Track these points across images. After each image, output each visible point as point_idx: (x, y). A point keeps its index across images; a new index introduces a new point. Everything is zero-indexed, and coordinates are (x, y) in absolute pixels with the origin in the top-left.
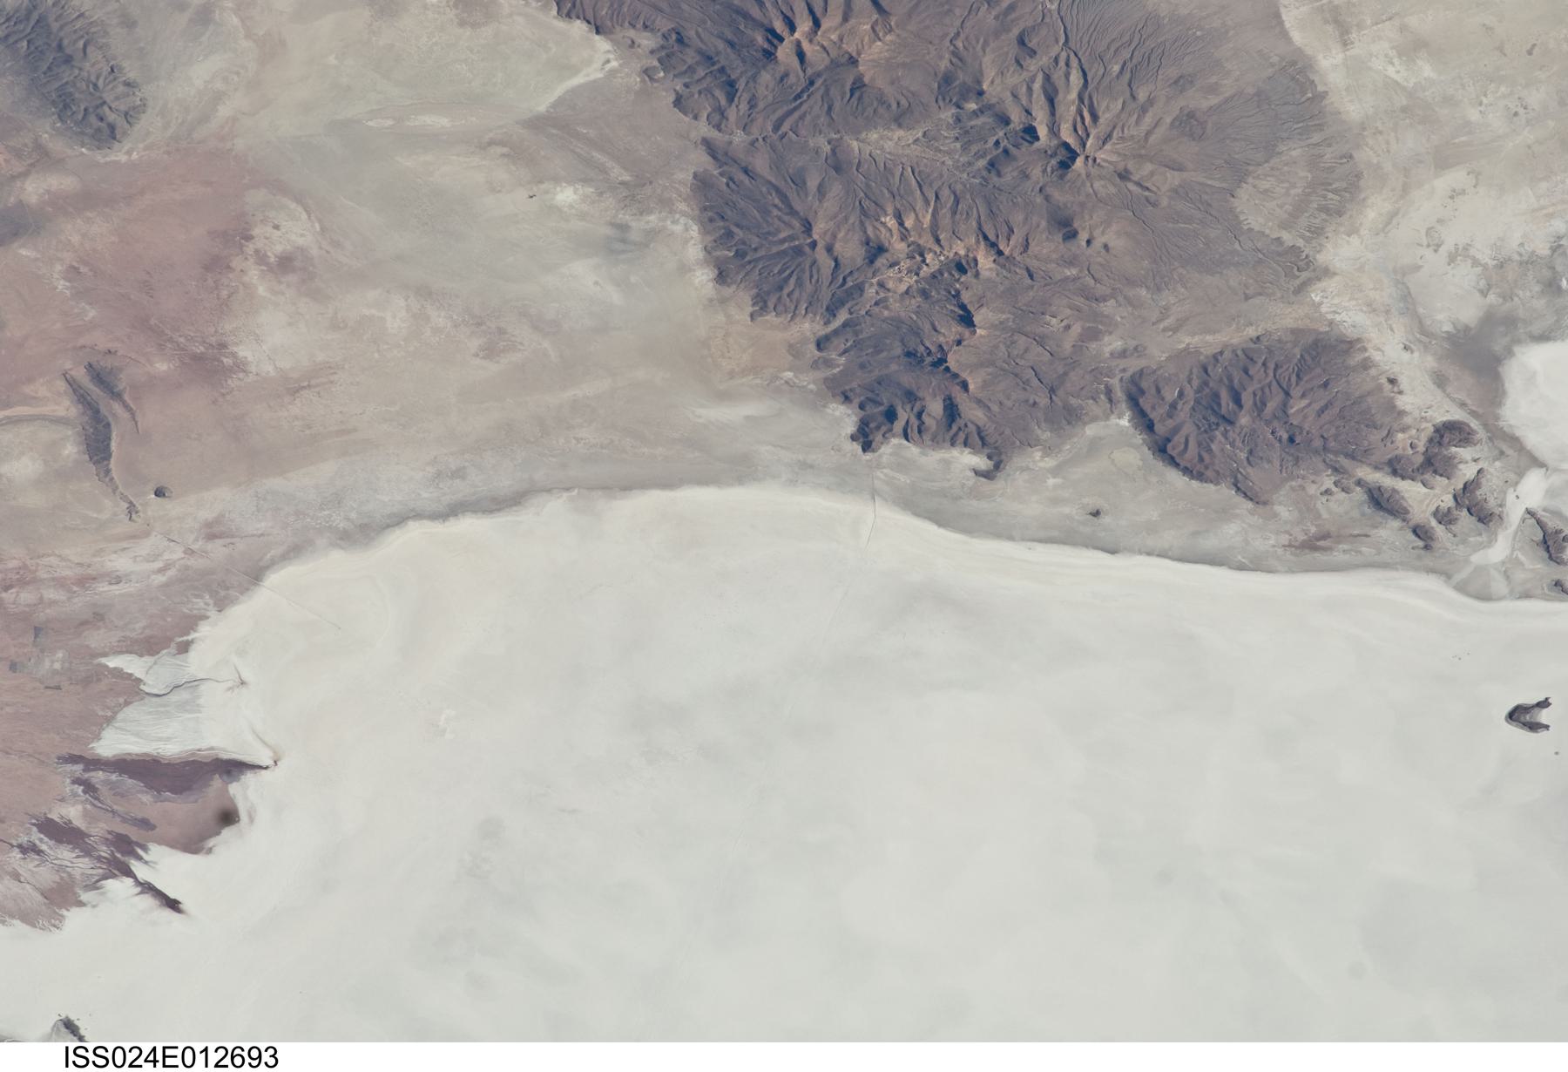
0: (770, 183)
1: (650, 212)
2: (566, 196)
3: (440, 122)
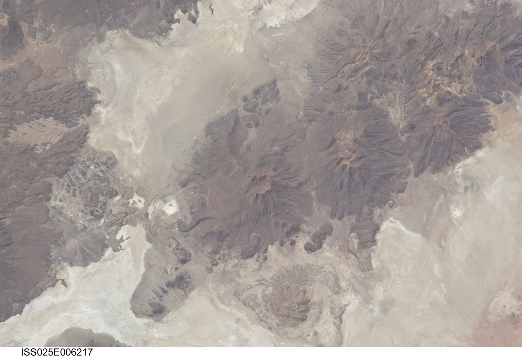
0: (426, 146)
1: (456, 182)
2: (457, 213)
3: (436, 269)
